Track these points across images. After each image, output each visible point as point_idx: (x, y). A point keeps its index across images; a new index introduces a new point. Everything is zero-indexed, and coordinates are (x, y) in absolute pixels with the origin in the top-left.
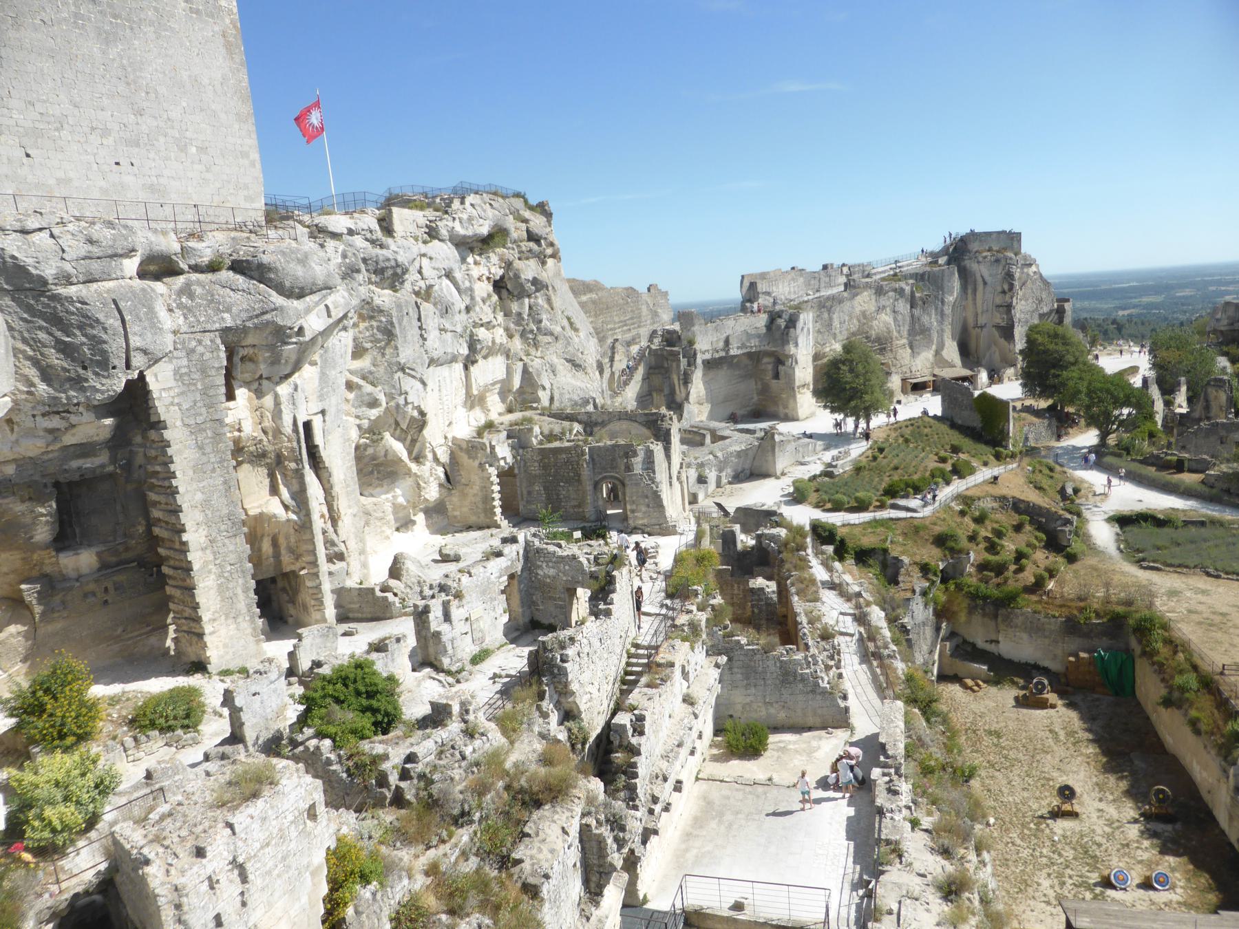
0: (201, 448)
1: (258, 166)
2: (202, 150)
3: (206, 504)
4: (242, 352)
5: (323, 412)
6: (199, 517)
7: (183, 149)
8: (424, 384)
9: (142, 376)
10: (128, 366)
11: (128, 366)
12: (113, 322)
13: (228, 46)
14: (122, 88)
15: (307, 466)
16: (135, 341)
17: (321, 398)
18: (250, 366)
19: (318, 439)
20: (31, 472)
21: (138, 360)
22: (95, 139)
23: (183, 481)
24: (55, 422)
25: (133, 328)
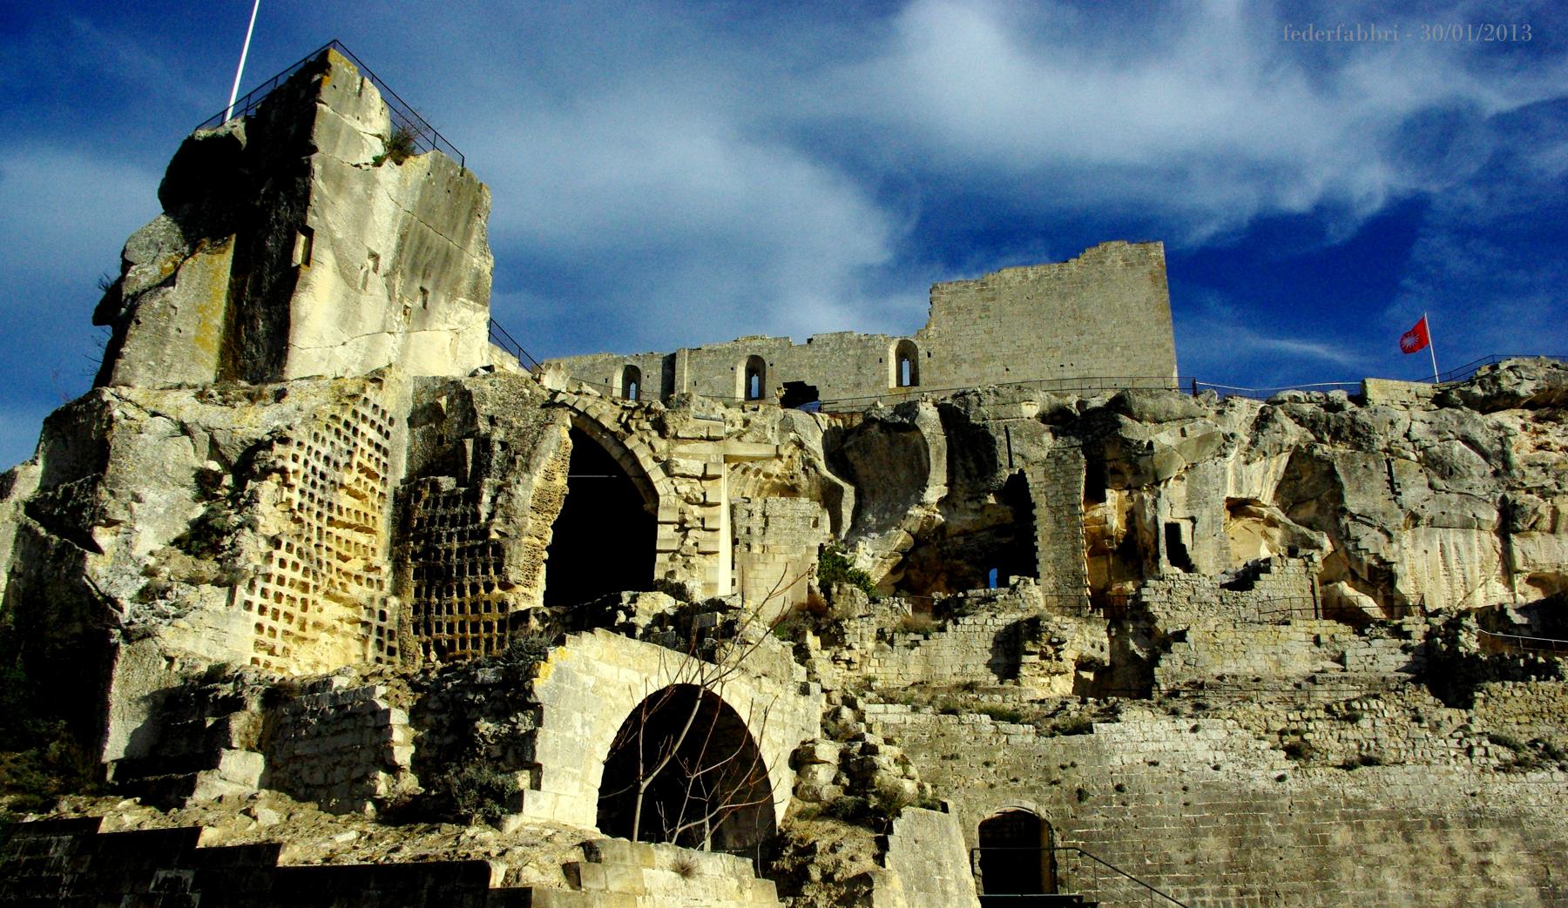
0: (1058, 522)
1: (1173, 351)
2: (1124, 348)
3: (1057, 561)
4: (1110, 465)
5: (1193, 519)
6: (1050, 568)
7: (1110, 349)
8: (1389, 535)
9: (1021, 472)
10: (1011, 465)
11: (1011, 465)
12: (1002, 438)
13: (1154, 280)
14: (1071, 322)
15: (1164, 557)
16: (1015, 449)
17: (1189, 506)
18: (1119, 477)
19: (1186, 539)
20: (1163, 687)
21: (1017, 461)
22: (1049, 354)
23: (1041, 543)
24: (974, 505)
25: (1015, 442)
